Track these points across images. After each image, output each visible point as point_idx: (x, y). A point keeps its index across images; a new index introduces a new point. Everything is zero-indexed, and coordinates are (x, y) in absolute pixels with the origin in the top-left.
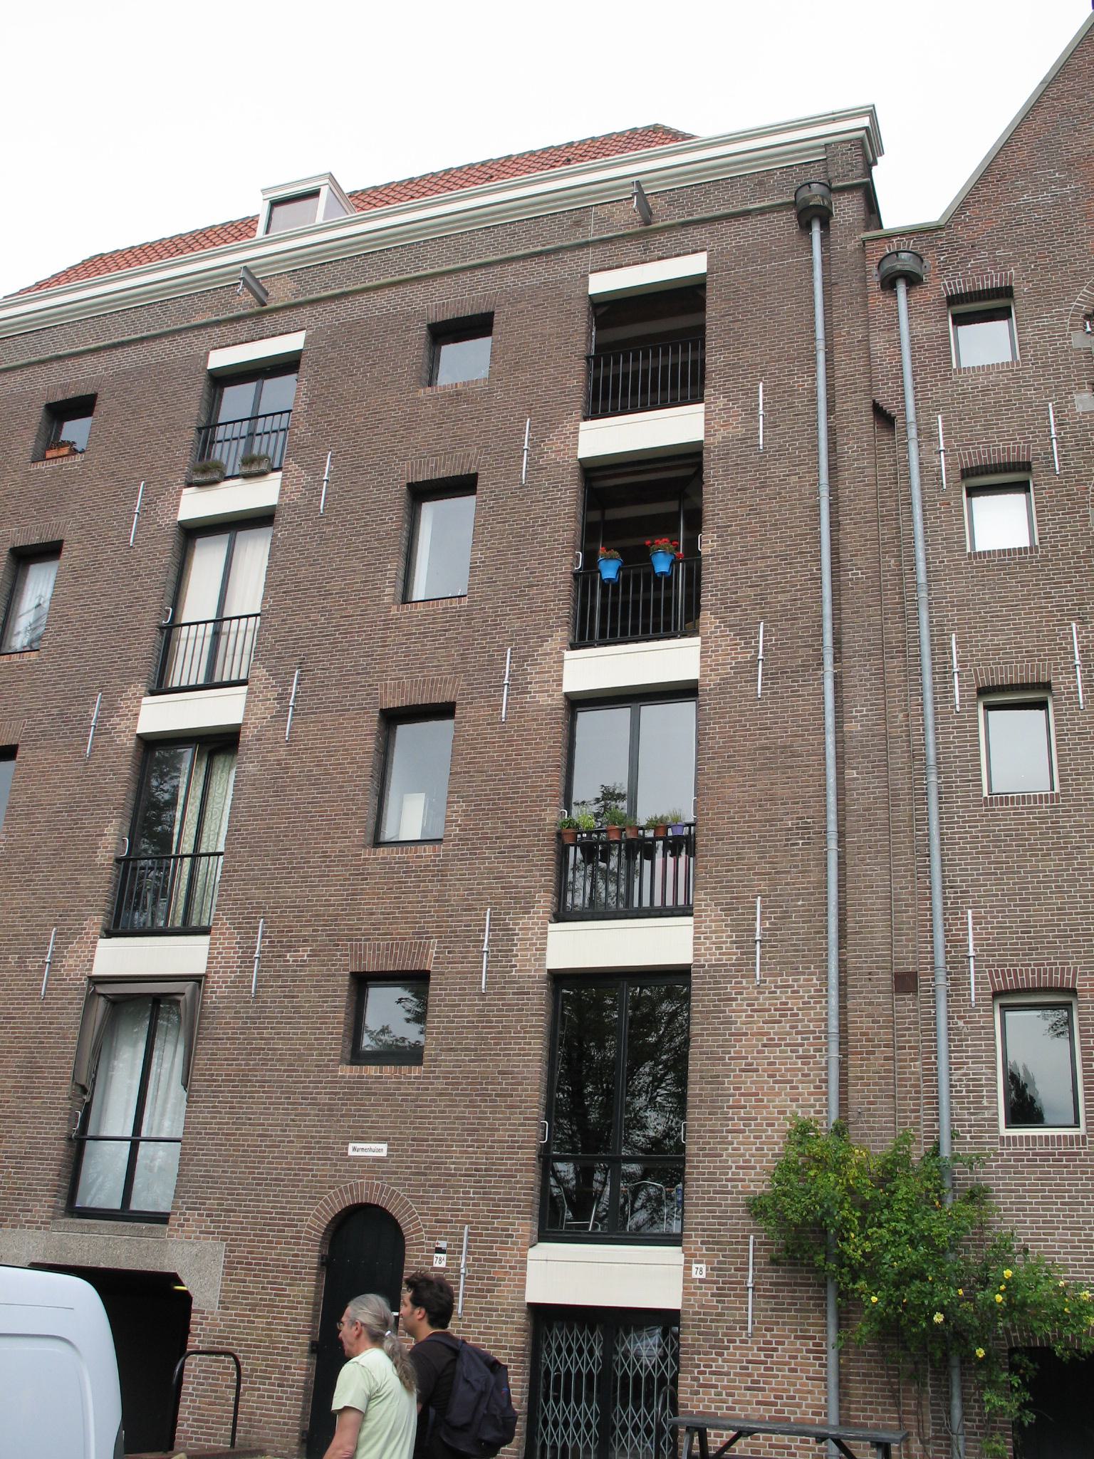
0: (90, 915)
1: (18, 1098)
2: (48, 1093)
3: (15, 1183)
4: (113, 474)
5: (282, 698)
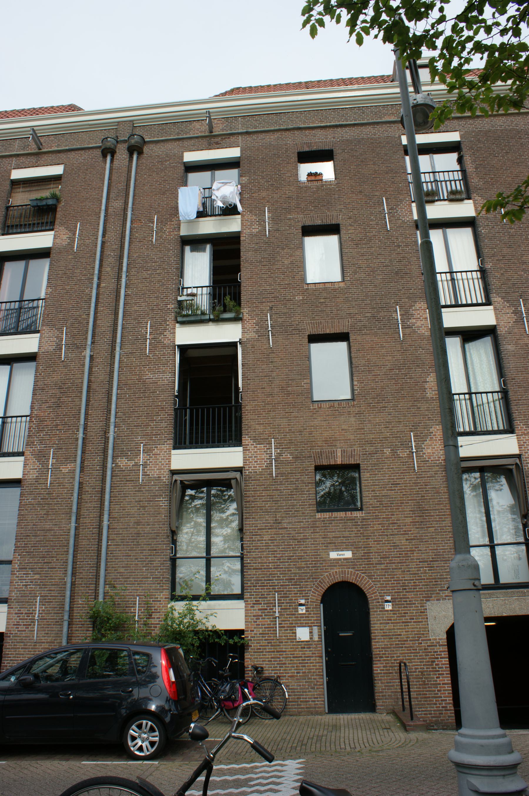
0: (433, 425)
1: (417, 528)
2: (437, 524)
3: (431, 576)
4: (361, 192)
5: (517, 312)
